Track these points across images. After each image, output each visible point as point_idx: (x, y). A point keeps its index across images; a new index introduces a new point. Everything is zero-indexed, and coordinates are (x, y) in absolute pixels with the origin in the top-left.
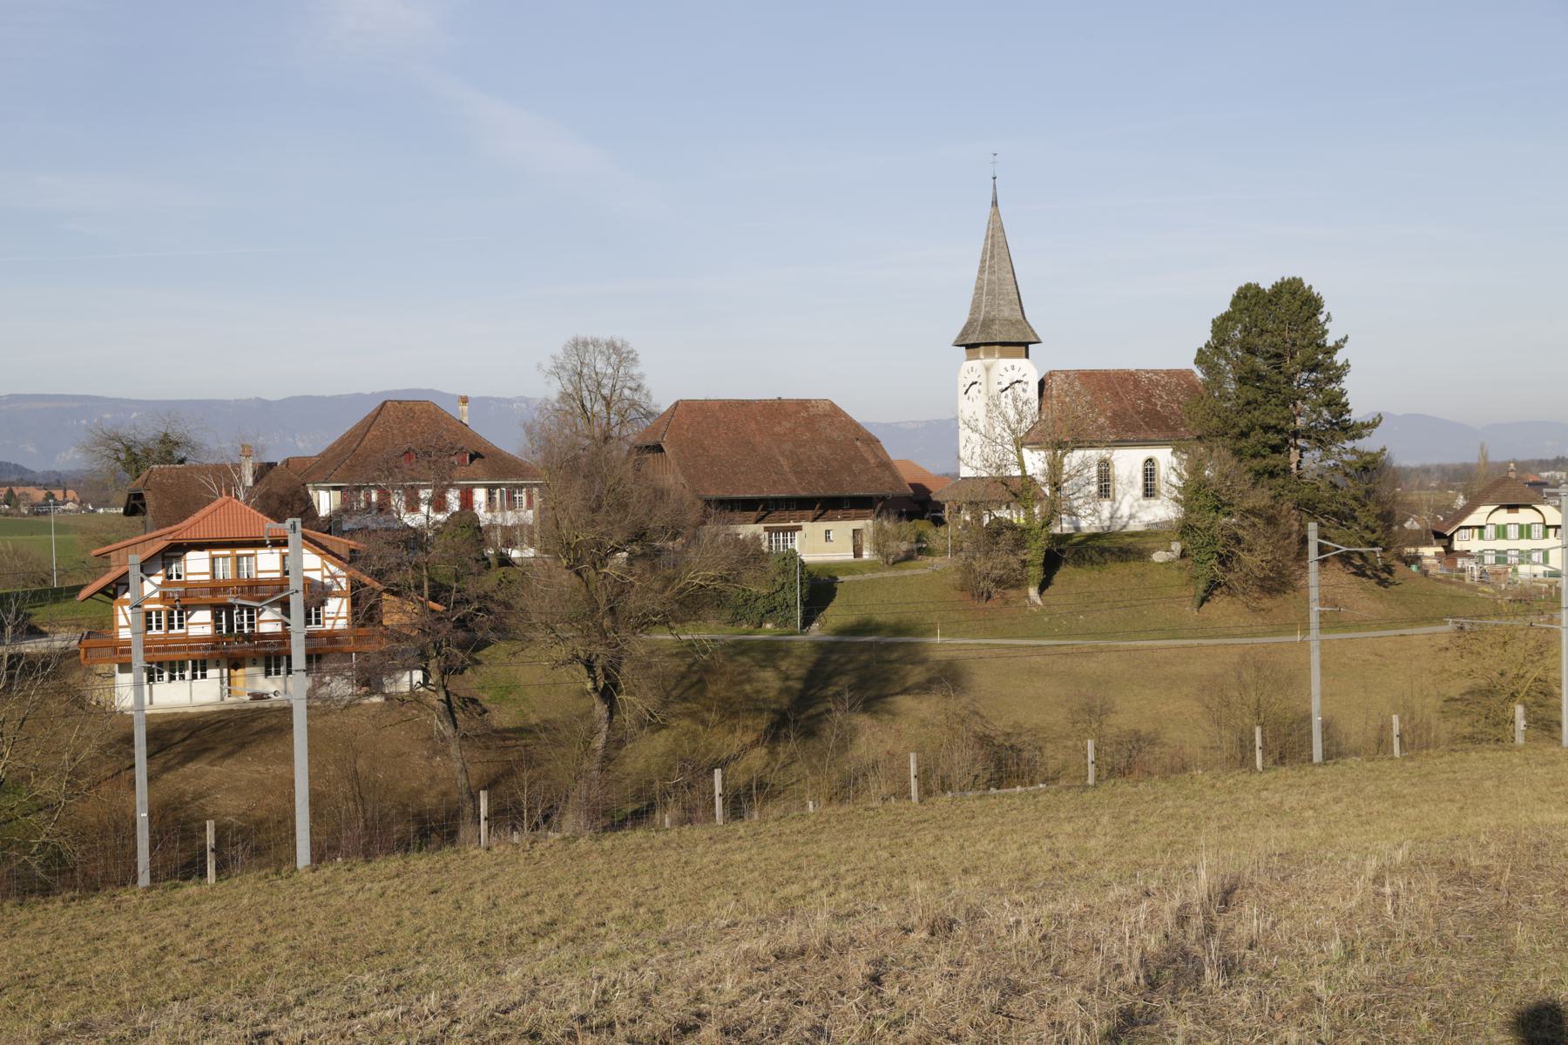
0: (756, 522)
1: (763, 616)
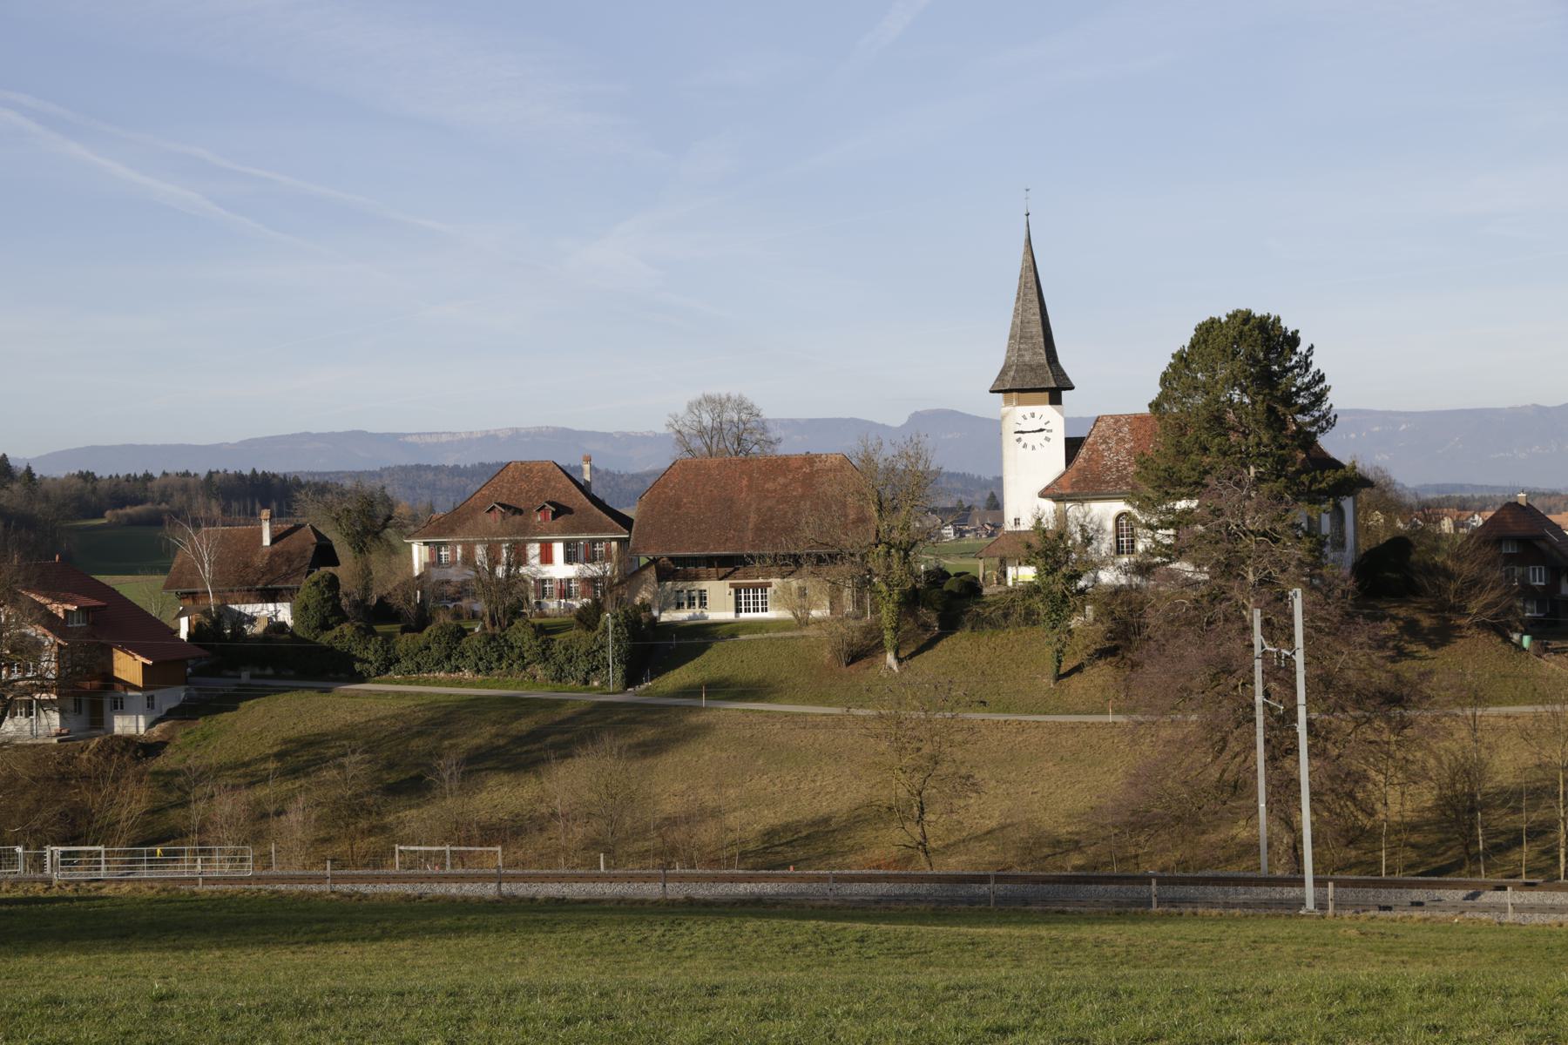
0: (721, 579)
1: (587, 673)
